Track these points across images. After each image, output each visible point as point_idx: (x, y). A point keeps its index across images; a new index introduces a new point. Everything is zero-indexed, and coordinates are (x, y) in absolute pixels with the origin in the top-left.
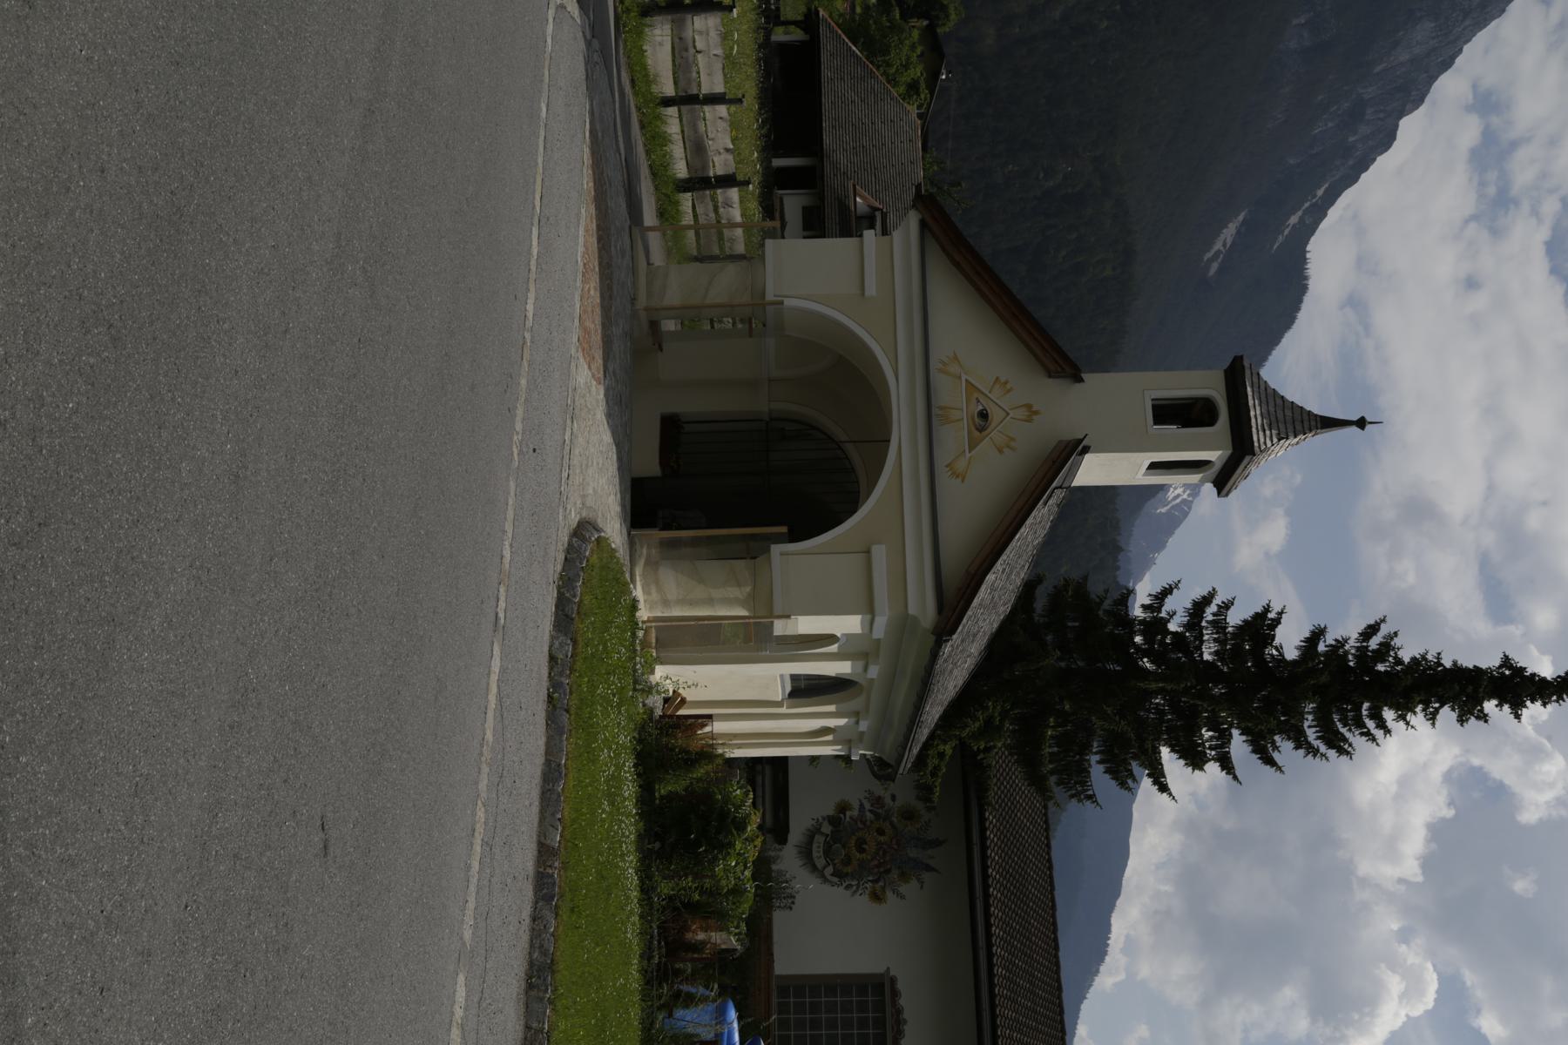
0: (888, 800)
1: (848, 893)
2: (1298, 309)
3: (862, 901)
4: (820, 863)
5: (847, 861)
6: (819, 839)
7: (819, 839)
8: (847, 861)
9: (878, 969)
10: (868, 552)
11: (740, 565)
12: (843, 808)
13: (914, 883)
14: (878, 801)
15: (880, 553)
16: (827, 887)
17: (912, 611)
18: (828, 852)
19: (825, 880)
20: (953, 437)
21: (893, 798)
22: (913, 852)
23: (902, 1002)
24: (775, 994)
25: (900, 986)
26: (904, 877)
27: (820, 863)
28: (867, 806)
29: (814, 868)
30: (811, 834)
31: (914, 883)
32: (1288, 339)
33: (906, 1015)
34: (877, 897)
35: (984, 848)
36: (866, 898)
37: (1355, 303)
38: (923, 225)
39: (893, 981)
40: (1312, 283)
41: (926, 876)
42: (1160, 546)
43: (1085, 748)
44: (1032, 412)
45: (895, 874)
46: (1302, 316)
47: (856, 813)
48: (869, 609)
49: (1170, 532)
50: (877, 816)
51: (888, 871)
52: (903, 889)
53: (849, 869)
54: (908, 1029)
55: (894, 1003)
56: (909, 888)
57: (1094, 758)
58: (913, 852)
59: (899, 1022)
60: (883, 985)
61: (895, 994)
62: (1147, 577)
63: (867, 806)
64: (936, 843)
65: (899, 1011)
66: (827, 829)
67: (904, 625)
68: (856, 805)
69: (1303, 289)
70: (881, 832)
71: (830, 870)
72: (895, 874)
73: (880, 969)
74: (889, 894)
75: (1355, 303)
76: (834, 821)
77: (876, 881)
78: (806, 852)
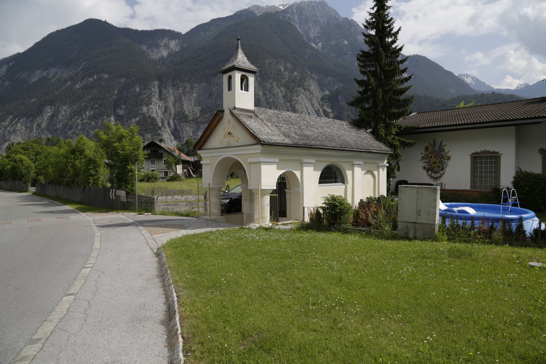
0: (423, 155)
1: (448, 167)
2: (422, 56)
3: (450, 162)
4: (439, 175)
5: (439, 167)
6: (433, 175)
7: (433, 175)
8: (439, 167)
9: (469, 159)
10: (250, 163)
11: (255, 197)
12: (424, 168)
13: (445, 147)
14: (423, 158)
15: (250, 160)
16: (446, 173)
17: (259, 151)
18: (436, 173)
19: (444, 173)
20: (233, 143)
21: (422, 153)
22: (437, 148)
23: (479, 151)
24: (475, 190)
25: (474, 152)
26: (443, 150)
27: (439, 175)
28: (424, 161)
29: (440, 176)
30: (431, 177)
31: (445, 147)
32: (429, 58)
33: (483, 150)
34: (449, 158)
35: (445, 126)
36: (449, 162)
37: (420, 43)
38: (200, 149)
39: (473, 154)
40: (415, 54)
41: (443, 144)
42: (484, 83)
43: (398, 100)
44: (229, 122)
45: (443, 153)
46: (423, 55)
47: (426, 164)
48: (260, 163)
49: (480, 81)
50: (427, 158)
51: (442, 155)
52: (447, 150)
53: (441, 166)
54: (487, 149)
55: (480, 153)
56: (447, 149)
57: (398, 97)
58: (437, 148)
59: (485, 152)
60: (474, 157)
61: (477, 153)
62: (492, 86)
63: (424, 161)
64: (434, 141)
65: (482, 152)
66: (430, 173)
67: (263, 153)
68: (424, 164)
69: (417, 55)
70: (431, 157)
71: (441, 172)
72: (443, 153)
73: (470, 157)
74: (448, 155)
75: (420, 43)
76: (428, 170)
77: (444, 159)
78: (436, 179)
